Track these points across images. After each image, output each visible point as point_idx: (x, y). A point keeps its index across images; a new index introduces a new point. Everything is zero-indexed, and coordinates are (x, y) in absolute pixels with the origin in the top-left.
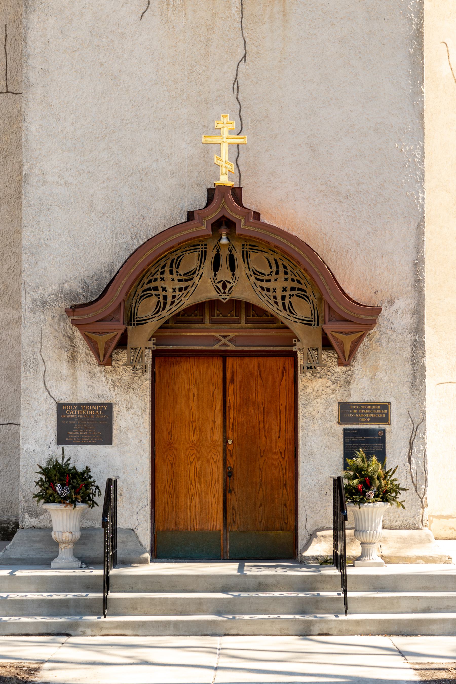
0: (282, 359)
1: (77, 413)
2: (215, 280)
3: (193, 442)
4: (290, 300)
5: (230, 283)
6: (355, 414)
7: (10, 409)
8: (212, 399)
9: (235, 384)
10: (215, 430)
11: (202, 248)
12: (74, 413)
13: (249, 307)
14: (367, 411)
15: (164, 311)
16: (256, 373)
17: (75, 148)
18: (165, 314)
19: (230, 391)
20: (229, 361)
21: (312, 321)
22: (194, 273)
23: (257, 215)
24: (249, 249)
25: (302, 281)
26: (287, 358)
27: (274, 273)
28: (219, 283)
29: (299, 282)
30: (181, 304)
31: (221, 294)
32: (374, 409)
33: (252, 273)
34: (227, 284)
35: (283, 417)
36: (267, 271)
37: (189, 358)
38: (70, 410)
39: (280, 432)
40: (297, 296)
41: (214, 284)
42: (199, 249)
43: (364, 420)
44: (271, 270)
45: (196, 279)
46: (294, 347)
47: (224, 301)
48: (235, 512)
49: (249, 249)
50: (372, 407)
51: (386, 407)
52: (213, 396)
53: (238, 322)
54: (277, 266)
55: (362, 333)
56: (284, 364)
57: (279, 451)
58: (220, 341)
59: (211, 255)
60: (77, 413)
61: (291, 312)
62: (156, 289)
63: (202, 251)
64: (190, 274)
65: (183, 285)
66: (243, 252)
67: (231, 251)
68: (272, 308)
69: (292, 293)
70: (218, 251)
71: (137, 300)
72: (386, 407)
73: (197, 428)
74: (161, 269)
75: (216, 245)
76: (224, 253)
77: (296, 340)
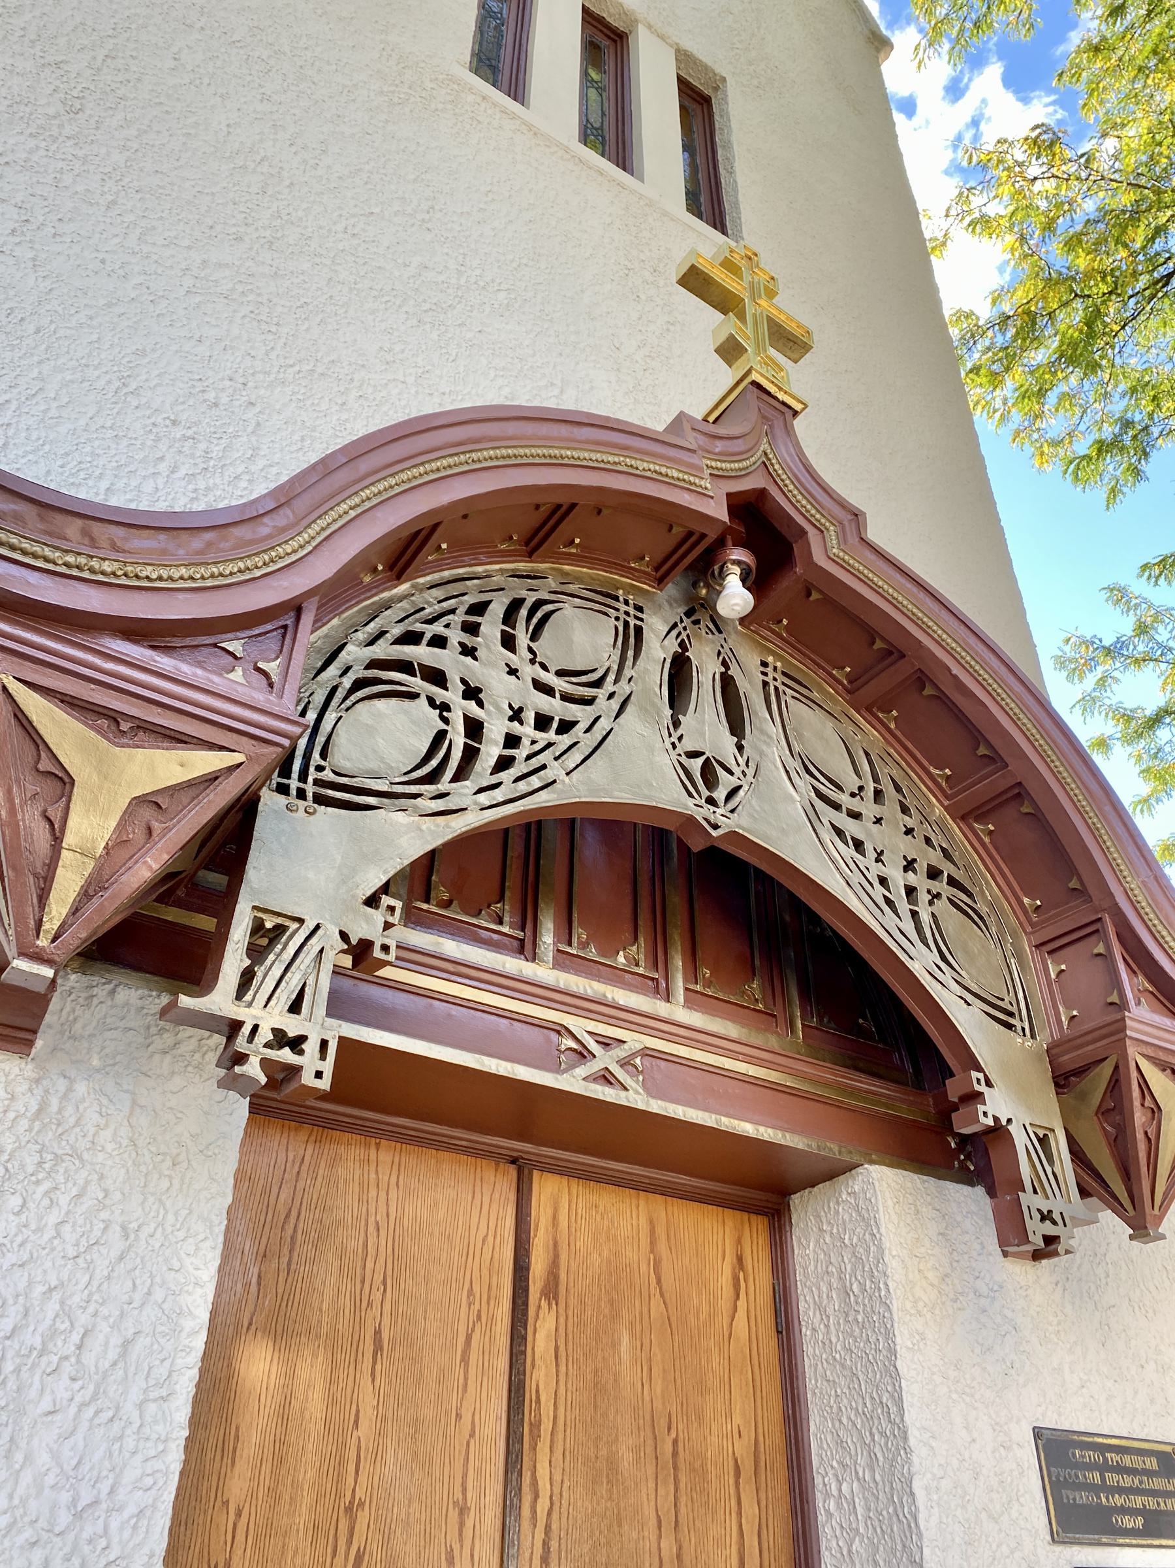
2: (674, 739)
8: (459, 1372)
15: (468, 786)
16: (644, 1268)
19: (541, 1336)
22: (598, 684)
26: (746, 1215)
36: (851, 782)
37: (378, 1145)
41: (674, 757)
42: (617, 610)
45: (604, 706)
52: (465, 1359)
56: (739, 1241)
62: (437, 677)
63: (626, 624)
64: (584, 679)
71: (334, 689)
74: (468, 612)
75: (675, 626)
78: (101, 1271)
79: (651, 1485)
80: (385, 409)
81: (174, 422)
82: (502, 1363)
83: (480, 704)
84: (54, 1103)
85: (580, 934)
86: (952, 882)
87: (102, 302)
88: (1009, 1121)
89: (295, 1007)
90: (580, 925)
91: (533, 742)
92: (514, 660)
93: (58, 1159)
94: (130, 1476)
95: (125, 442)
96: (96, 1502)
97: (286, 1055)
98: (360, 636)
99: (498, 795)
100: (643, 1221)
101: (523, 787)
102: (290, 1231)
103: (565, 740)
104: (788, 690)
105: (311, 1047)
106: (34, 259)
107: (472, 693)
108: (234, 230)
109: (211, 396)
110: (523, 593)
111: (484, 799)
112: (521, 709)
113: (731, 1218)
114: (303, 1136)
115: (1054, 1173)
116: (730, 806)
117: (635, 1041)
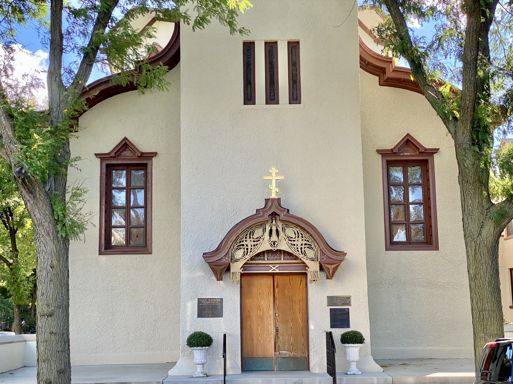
0: (300, 276)
5: (277, 242)
6: (335, 301)
7: (169, 299)
13: (285, 252)
18: (248, 257)
20: (276, 277)
22: (260, 238)
23: (288, 210)
25: (310, 241)
27: (297, 237)
28: (272, 242)
29: (308, 241)
33: (287, 238)
35: (301, 302)
36: (294, 236)
45: (261, 240)
51: (349, 298)
52: (269, 294)
53: (280, 259)
54: (298, 234)
55: (338, 264)
58: (272, 268)
59: (268, 229)
61: (305, 255)
62: (243, 245)
65: (255, 243)
66: (283, 228)
67: (277, 228)
68: (297, 254)
69: (305, 246)
70: (271, 228)
72: (349, 298)
73: (262, 309)
76: (274, 229)
100: (288, 278)
109: (221, 205)
111: (250, 256)
114: (249, 277)
117: (277, 266)
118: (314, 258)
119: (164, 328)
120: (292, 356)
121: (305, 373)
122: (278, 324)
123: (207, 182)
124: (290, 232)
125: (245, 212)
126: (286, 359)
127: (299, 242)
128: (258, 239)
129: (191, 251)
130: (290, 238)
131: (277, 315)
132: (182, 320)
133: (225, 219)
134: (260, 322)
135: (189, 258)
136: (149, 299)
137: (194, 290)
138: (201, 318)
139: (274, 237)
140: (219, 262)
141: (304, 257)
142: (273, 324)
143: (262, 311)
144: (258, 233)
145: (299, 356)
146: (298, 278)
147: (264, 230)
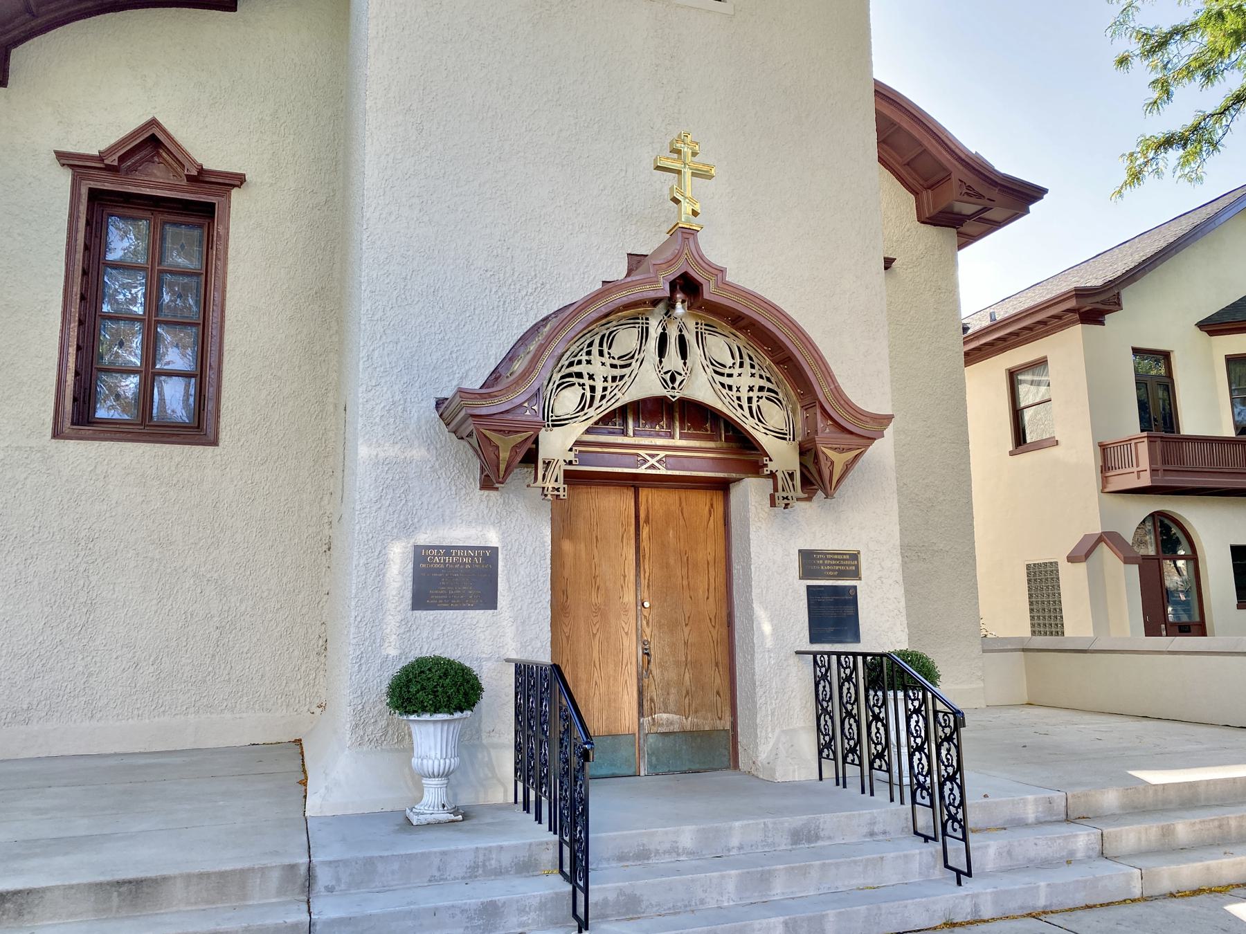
1: (445, 560)
2: (660, 369)
3: (596, 605)
4: (759, 403)
5: (681, 375)
6: (820, 565)
9: (650, 526)
10: (625, 589)
11: (643, 323)
12: (440, 560)
14: (834, 562)
17: (445, 173)
18: (594, 414)
20: (643, 493)
21: (786, 434)
22: (632, 357)
24: (705, 329)
27: (738, 364)
28: (666, 373)
30: (613, 401)
31: (669, 390)
32: (841, 559)
34: (675, 374)
36: (729, 362)
38: (434, 556)
39: (708, 590)
40: (767, 398)
41: (659, 375)
42: (639, 323)
43: (831, 573)
44: (734, 361)
45: (635, 365)
46: (765, 469)
47: (673, 400)
48: (655, 705)
49: (705, 329)
50: (839, 557)
51: (855, 556)
52: (622, 542)
55: (860, 450)
56: (712, 499)
57: (708, 618)
60: (445, 560)
62: (579, 375)
63: (642, 327)
64: (627, 357)
65: (617, 372)
66: (697, 333)
67: (681, 331)
69: (760, 394)
72: (855, 556)
73: (602, 585)
75: (661, 321)
76: (673, 334)
77: (768, 458)
78: (525, 535)
79: (680, 568)
80: (554, 225)
81: (486, 271)
82: (633, 542)
83: (594, 380)
84: (507, 501)
85: (642, 421)
86: (769, 390)
87: (453, 226)
88: (777, 471)
89: (556, 481)
90: (643, 419)
91: (611, 387)
92: (603, 360)
93: (510, 512)
94: (540, 575)
95: (474, 287)
96: (535, 580)
97: (556, 493)
98: (557, 369)
99: (602, 409)
100: (677, 498)
101: (609, 403)
102: (569, 514)
103: (622, 382)
104: (706, 332)
105: (561, 490)
106: (429, 220)
107: (591, 377)
108: (486, 160)
110: (605, 332)
111: (599, 411)
112: (607, 377)
113: (709, 493)
115: (793, 485)
116: (680, 388)
117: (662, 454)
118: (784, 431)
119: (245, 650)
120: (688, 728)
121: (727, 776)
122: (648, 631)
123: (451, 178)
124: (720, 347)
125: (568, 285)
126: (672, 737)
127: (744, 380)
128: (627, 360)
129: (396, 387)
130: (718, 368)
131: (647, 604)
132: (359, 619)
133: (508, 301)
134: (597, 626)
135: (389, 410)
136: (203, 569)
137: (402, 518)
138: (425, 612)
139: (673, 360)
140: (509, 417)
141: (756, 427)
142: (634, 631)
143: (603, 592)
144: (627, 340)
145: (707, 728)
146: (700, 501)
147: (645, 334)
